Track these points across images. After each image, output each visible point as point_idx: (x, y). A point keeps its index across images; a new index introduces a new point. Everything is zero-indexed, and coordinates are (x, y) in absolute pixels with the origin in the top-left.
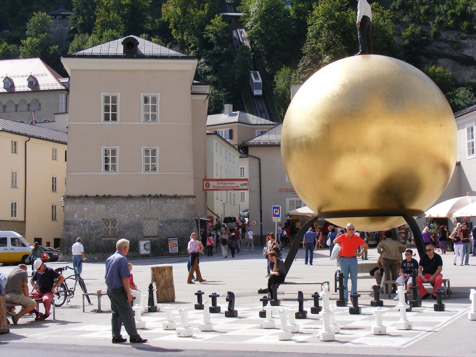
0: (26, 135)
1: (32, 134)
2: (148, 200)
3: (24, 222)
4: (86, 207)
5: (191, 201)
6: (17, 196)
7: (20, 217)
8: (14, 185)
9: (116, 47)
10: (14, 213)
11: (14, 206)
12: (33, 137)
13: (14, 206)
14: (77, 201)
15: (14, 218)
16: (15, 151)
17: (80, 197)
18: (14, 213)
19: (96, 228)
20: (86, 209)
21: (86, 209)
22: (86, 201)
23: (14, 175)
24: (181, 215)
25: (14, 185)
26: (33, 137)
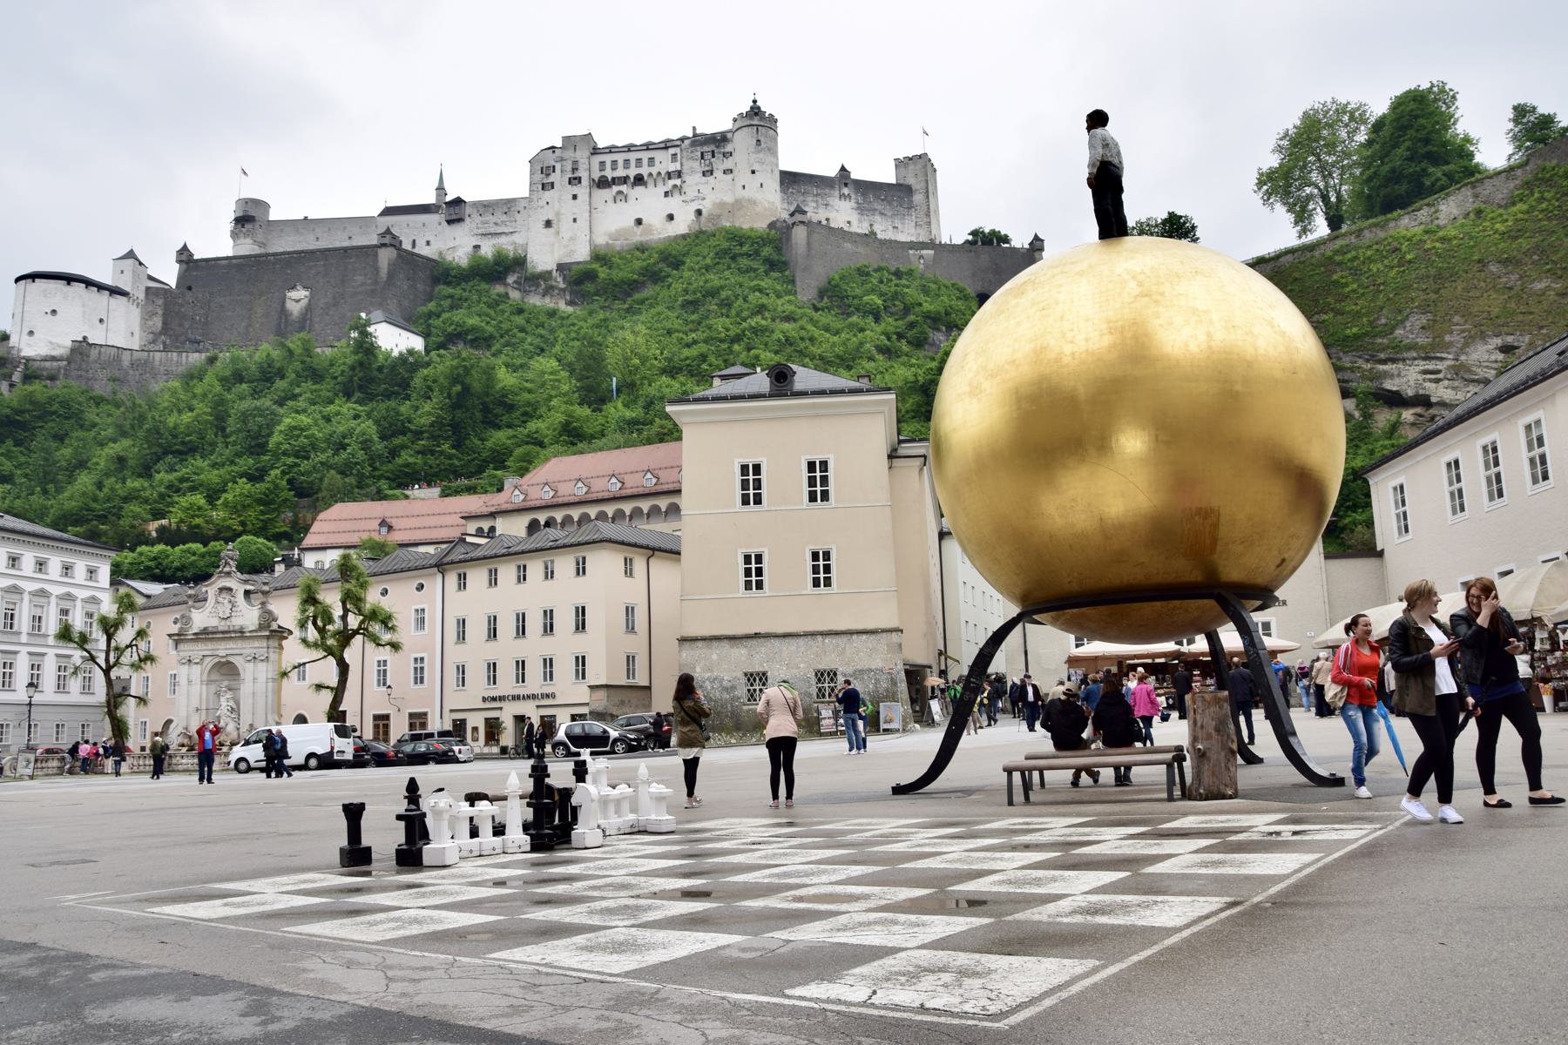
0: (647, 547)
1: (656, 545)
2: (820, 638)
3: (649, 688)
4: (716, 653)
5: (895, 637)
6: (637, 644)
7: (641, 680)
8: (630, 628)
9: (760, 381)
10: (630, 672)
11: (630, 660)
12: (660, 550)
13: (630, 660)
14: (700, 644)
15: (631, 682)
16: (629, 573)
17: (704, 639)
18: (630, 672)
19: (733, 688)
20: (715, 657)
21: (715, 657)
22: (715, 644)
23: (630, 611)
24: (877, 663)
25: (630, 628)
26: (660, 550)
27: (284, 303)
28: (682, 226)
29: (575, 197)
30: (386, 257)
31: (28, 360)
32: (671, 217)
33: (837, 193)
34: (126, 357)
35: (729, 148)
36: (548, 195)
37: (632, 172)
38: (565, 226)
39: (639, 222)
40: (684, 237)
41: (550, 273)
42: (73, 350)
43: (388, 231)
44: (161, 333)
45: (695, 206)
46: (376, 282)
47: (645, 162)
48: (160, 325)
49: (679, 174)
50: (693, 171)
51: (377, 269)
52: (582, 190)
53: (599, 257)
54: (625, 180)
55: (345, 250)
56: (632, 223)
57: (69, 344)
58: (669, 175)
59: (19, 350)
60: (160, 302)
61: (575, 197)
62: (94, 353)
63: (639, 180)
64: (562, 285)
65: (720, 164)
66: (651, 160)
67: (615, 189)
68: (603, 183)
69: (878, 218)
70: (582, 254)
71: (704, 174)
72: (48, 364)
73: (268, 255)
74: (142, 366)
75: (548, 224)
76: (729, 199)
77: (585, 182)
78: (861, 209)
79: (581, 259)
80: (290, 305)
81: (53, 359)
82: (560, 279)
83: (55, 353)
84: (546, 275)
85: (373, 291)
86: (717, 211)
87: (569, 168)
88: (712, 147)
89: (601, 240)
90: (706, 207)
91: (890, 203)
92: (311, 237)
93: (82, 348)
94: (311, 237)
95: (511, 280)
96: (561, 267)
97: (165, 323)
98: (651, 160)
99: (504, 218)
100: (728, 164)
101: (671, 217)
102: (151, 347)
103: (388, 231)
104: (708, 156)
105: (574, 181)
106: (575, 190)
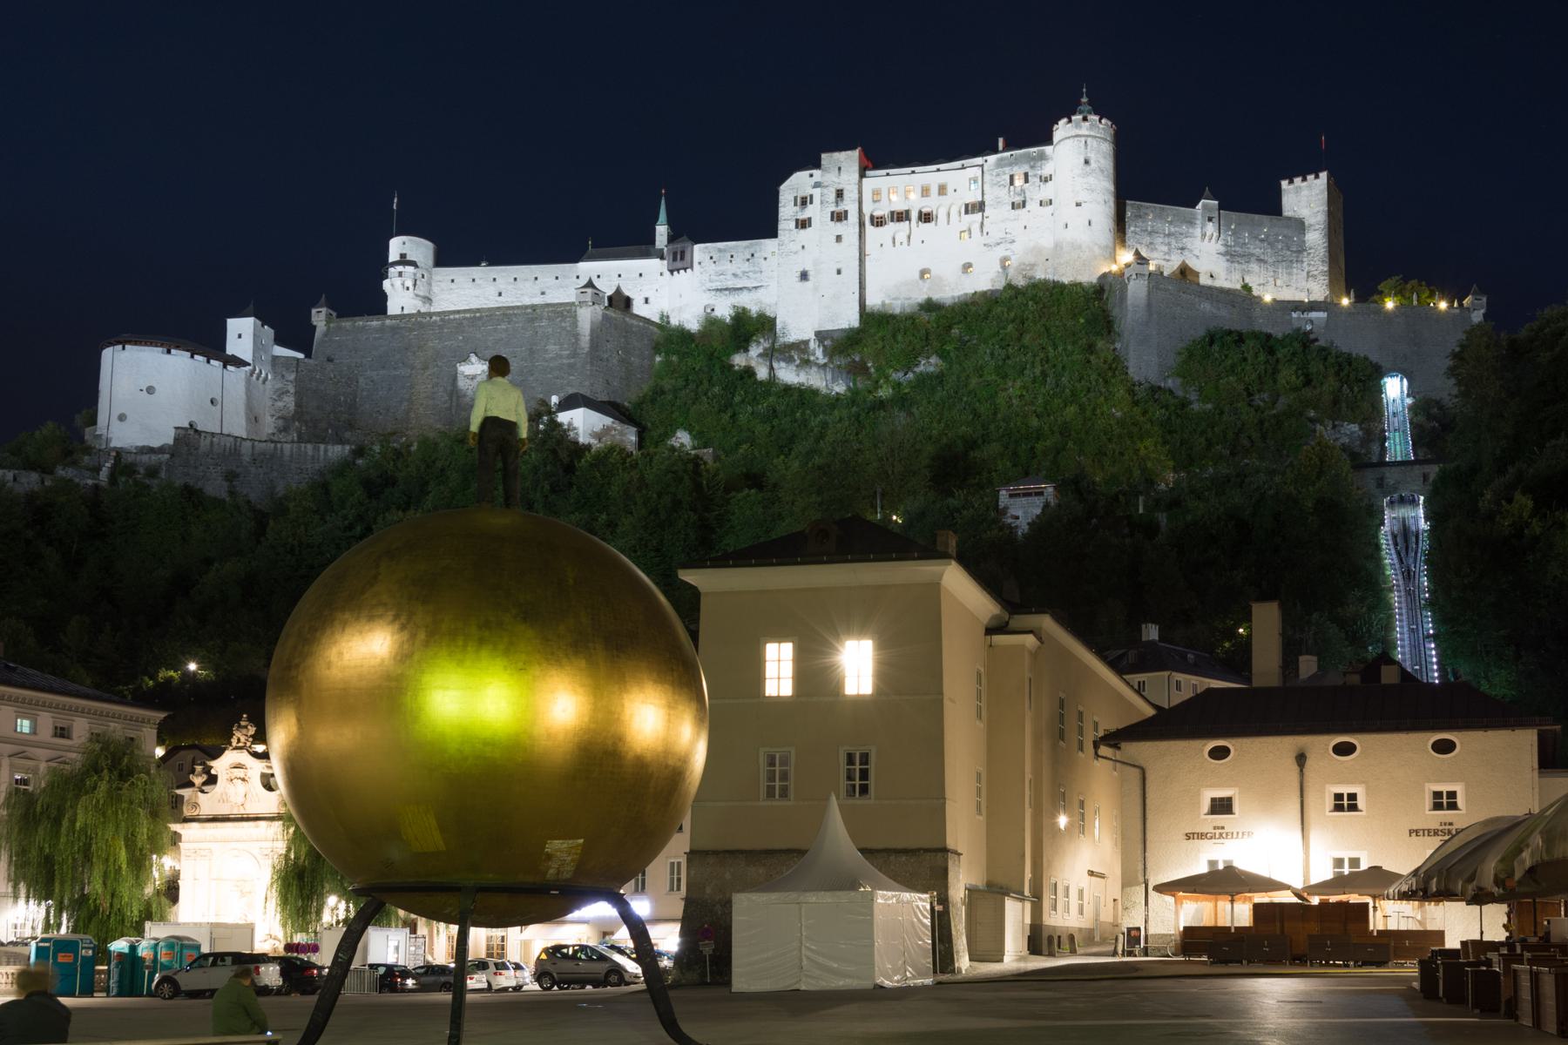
27: (455, 379)
28: (985, 279)
29: (839, 239)
30: (587, 317)
31: (119, 452)
32: (967, 267)
33: (1198, 232)
34: (246, 448)
35: (1047, 169)
36: (804, 234)
37: (915, 203)
38: (823, 278)
39: (923, 273)
40: (984, 294)
41: (806, 343)
42: (176, 439)
43: (590, 284)
44: (293, 418)
45: (1001, 252)
46: (574, 355)
47: (934, 190)
48: (292, 406)
49: (980, 207)
50: (999, 203)
51: (577, 336)
52: (849, 229)
53: (875, 322)
54: (902, 216)
55: (534, 307)
56: (917, 275)
57: (172, 433)
58: (970, 209)
59: (108, 441)
60: (292, 377)
61: (839, 239)
62: (204, 443)
63: (926, 218)
64: (822, 360)
65: (1036, 192)
66: (942, 190)
67: (891, 227)
68: (878, 222)
69: (1254, 266)
70: (849, 318)
71: (1014, 206)
72: (145, 458)
73: (430, 315)
74: (267, 459)
75: (804, 276)
76: (1047, 242)
77: (853, 217)
78: (1231, 255)
79: (845, 325)
80: (462, 384)
81: (151, 450)
82: (819, 353)
83: (156, 443)
84: (801, 346)
85: (571, 366)
86: (1031, 260)
87: (832, 196)
88: (1026, 168)
89: (874, 300)
90: (1018, 255)
91: (1271, 245)
92: (491, 290)
93: (188, 437)
94: (491, 290)
95: (755, 351)
96: (821, 336)
97: (298, 405)
98: (942, 190)
99: (746, 266)
100: (1047, 191)
101: (967, 267)
102: (281, 437)
103: (590, 284)
104: (1019, 182)
105: (839, 217)
106: (839, 228)
